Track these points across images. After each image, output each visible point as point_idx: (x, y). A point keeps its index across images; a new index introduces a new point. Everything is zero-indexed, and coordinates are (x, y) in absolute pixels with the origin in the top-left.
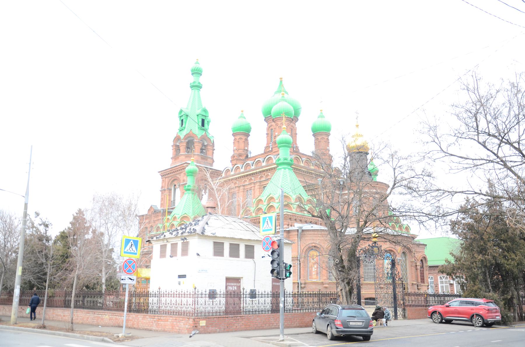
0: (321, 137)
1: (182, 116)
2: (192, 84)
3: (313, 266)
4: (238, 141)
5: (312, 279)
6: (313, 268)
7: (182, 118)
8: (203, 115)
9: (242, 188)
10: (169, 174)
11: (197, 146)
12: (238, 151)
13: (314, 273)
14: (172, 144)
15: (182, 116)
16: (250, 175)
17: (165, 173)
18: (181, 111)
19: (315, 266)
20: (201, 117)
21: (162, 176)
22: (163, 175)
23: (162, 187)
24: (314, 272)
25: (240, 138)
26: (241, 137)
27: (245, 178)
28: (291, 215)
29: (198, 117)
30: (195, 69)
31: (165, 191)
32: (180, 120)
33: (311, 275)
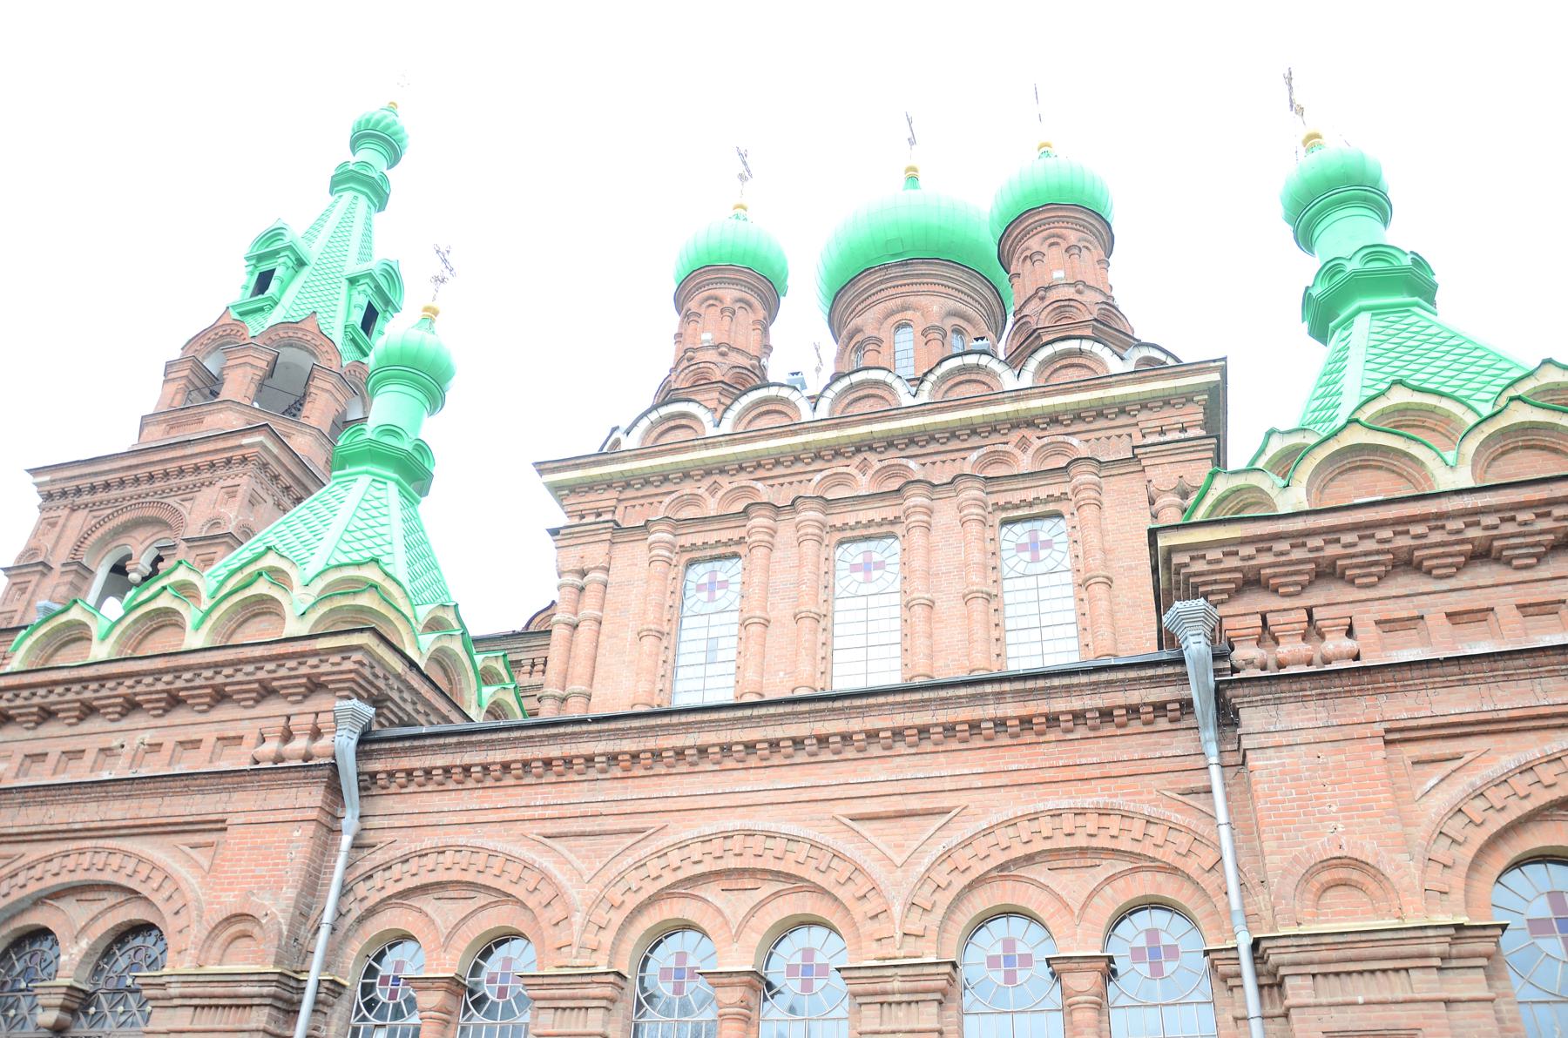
1: (275, 253)
2: (351, 167)
7: (265, 267)
8: (378, 289)
9: (810, 514)
10: (107, 486)
11: (327, 395)
12: (723, 354)
14: (176, 354)
15: (275, 253)
16: (890, 442)
17: (84, 483)
18: (275, 234)
20: (370, 292)
21: (49, 496)
22: (64, 494)
23: (31, 551)
25: (740, 300)
26: (748, 297)
27: (841, 461)
29: (350, 290)
31: (43, 575)
32: (252, 273)
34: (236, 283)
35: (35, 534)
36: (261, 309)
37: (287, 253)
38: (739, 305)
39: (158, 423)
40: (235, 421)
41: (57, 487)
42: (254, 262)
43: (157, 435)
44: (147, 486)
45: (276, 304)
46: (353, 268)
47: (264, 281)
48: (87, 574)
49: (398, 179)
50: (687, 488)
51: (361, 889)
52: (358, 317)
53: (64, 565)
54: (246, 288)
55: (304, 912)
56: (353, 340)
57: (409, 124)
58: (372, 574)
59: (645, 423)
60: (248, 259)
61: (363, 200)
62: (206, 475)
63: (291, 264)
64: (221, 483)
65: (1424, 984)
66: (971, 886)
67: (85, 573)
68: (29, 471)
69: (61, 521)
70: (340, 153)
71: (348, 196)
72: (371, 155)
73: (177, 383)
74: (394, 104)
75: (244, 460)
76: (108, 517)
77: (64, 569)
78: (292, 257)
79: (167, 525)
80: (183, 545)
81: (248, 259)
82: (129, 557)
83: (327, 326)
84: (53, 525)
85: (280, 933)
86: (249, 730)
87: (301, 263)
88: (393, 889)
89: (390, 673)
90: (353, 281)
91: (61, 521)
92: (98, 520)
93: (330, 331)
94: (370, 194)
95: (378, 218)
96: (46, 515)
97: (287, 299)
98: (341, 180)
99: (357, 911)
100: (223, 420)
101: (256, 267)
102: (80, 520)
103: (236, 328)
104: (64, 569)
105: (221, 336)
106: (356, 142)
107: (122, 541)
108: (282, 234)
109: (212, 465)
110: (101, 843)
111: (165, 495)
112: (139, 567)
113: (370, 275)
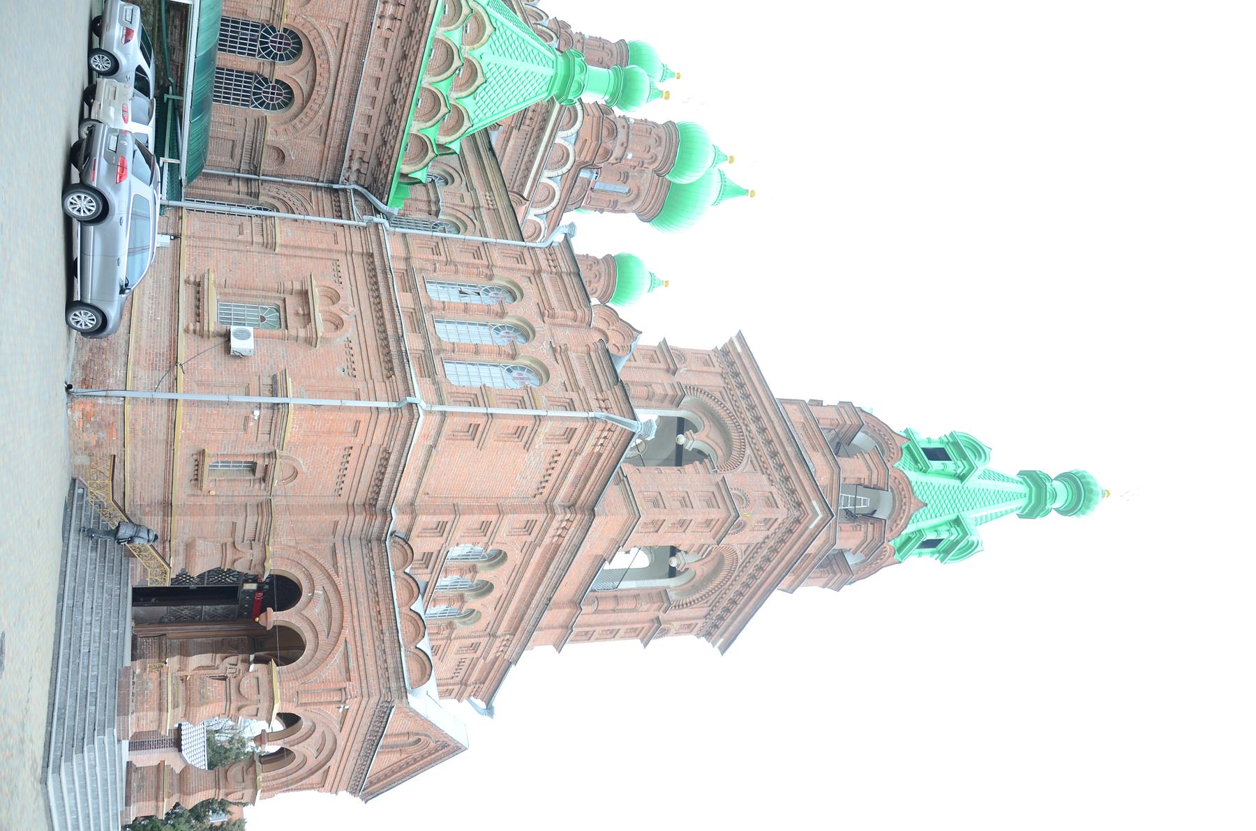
1: (964, 457)
2: (1048, 485)
10: (747, 396)
15: (964, 456)
18: (978, 450)
23: (682, 355)
31: (668, 370)
32: (942, 442)
34: (930, 433)
35: (696, 353)
36: (916, 462)
37: (967, 467)
39: (802, 413)
40: (823, 479)
41: (733, 356)
42: (951, 440)
43: (795, 415)
44: (750, 417)
45: (925, 472)
46: (968, 518)
47: (936, 454)
48: (675, 403)
49: (1052, 522)
52: (931, 536)
53: (679, 384)
54: (929, 440)
57: (1100, 511)
61: (1023, 502)
62: (777, 476)
63: (958, 472)
64: (774, 490)
67: (676, 402)
68: (740, 331)
69: (712, 369)
70: (1053, 469)
71: (1023, 489)
72: (1063, 494)
73: (838, 417)
74: (1109, 494)
75: (799, 504)
76: (727, 409)
77: (676, 386)
78: (966, 470)
79: (729, 453)
80: (719, 479)
82: (696, 431)
83: (918, 516)
84: (706, 363)
87: (962, 478)
90: (957, 522)
91: (712, 369)
92: (721, 400)
93: (915, 521)
94: (1031, 504)
95: (1014, 515)
96: (712, 355)
98: (1035, 480)
100: (818, 461)
101: (947, 444)
102: (712, 382)
103: (895, 451)
104: (676, 386)
105: (884, 439)
106: (1068, 478)
107: (706, 423)
108: (980, 455)
109: (787, 479)
111: (753, 445)
112: (691, 442)
113: (965, 534)
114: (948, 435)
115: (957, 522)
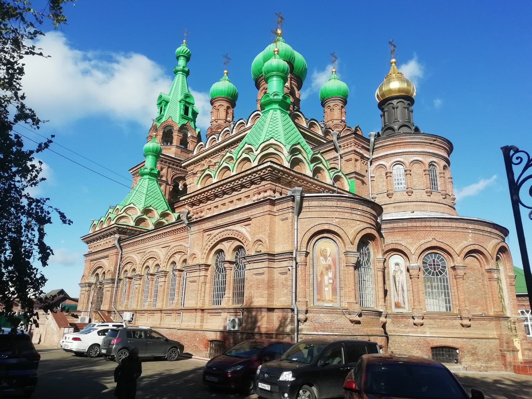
0: (334, 103)
3: (324, 273)
4: (217, 108)
5: (323, 301)
6: (326, 278)
7: (161, 106)
12: (216, 122)
13: (326, 289)
18: (161, 97)
19: (330, 275)
24: (327, 286)
28: (279, 171)
30: (180, 51)
33: (320, 291)
38: (220, 106)
50: (203, 162)
51: (122, 264)
52: (182, 112)
55: (115, 269)
56: (183, 118)
58: (132, 205)
59: (196, 148)
60: (157, 105)
65: (197, 274)
66: (170, 258)
81: (157, 105)
85: (112, 273)
86: (111, 240)
88: (125, 263)
89: (124, 228)
90: (180, 102)
97: (165, 115)
99: (122, 267)
110: (98, 261)
113: (182, 100)
114: (157, 106)
115: (180, 102)
